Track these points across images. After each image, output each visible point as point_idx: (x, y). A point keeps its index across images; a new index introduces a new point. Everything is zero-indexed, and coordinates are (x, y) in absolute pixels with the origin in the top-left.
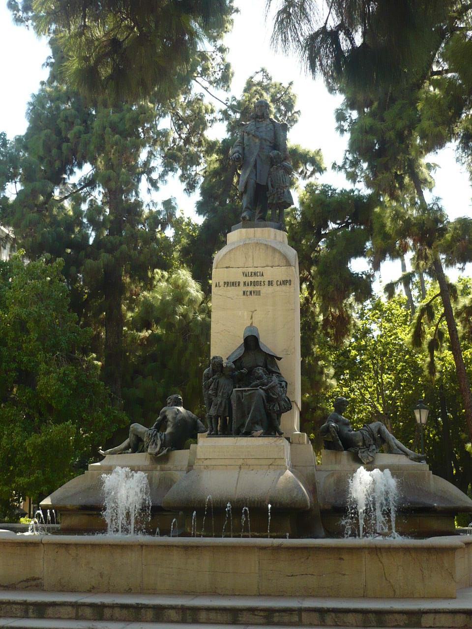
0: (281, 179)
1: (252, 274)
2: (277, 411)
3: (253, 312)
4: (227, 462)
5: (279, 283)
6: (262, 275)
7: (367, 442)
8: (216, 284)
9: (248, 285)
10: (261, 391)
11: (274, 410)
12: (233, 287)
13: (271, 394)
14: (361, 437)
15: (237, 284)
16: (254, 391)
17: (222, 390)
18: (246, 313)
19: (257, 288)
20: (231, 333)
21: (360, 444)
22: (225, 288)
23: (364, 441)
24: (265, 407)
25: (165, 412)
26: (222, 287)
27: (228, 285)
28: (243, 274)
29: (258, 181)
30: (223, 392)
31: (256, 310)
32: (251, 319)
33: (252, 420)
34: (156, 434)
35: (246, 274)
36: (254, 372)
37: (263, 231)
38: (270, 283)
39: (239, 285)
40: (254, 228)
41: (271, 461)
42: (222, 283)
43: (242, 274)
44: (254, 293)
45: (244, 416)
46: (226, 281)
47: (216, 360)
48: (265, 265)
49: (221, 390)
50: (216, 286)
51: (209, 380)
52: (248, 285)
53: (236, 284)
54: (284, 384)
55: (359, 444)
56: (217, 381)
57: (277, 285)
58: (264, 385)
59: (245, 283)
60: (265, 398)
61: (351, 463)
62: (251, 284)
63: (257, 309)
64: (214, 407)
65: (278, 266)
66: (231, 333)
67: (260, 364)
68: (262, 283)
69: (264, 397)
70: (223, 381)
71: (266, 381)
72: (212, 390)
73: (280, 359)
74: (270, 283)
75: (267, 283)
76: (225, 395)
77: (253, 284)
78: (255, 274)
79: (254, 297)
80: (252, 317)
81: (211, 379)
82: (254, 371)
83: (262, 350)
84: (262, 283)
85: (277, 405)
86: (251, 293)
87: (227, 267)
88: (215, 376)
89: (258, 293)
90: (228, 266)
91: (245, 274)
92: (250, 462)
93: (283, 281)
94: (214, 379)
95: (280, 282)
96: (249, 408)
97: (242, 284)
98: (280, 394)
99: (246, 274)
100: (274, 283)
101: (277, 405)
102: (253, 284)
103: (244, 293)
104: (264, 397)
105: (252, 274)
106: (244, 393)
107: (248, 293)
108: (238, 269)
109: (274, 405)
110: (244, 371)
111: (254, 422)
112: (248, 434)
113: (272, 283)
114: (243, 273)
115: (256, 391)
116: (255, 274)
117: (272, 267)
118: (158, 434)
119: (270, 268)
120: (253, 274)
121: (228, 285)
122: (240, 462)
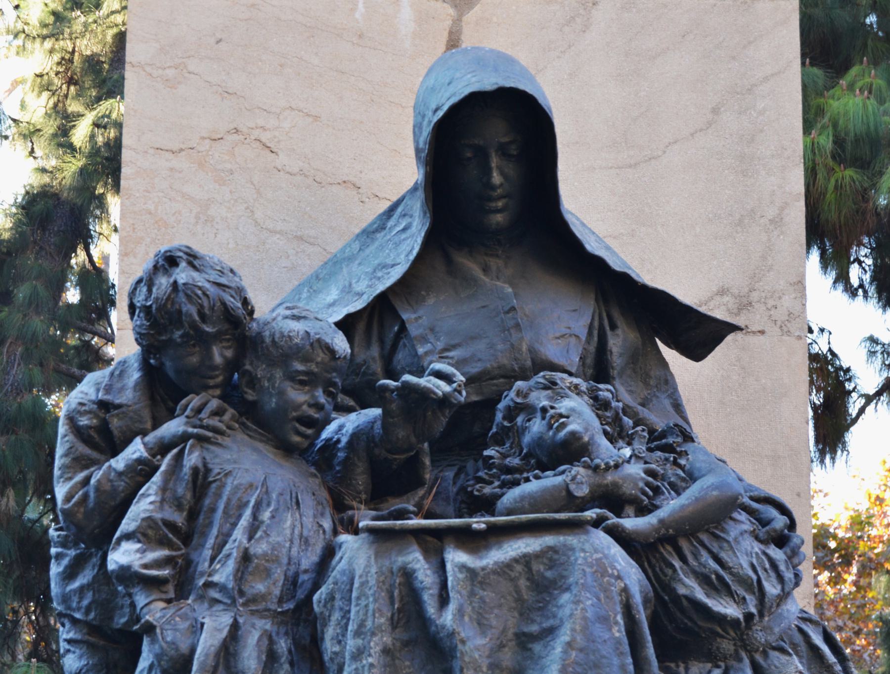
16: (550, 540)
17: (239, 534)
20: (282, 160)
30: (246, 557)
36: (512, 412)
47: (183, 274)
49: (224, 539)
51: (119, 463)
54: (780, 522)
56: (192, 459)
66: (282, 160)
67: (552, 351)
69: (637, 599)
71: (635, 470)
76: (260, 587)
81: (136, 449)
82: (510, 397)
88: (173, 427)
98: (772, 589)
104: (637, 599)
106: (456, 557)
115: (571, 540)
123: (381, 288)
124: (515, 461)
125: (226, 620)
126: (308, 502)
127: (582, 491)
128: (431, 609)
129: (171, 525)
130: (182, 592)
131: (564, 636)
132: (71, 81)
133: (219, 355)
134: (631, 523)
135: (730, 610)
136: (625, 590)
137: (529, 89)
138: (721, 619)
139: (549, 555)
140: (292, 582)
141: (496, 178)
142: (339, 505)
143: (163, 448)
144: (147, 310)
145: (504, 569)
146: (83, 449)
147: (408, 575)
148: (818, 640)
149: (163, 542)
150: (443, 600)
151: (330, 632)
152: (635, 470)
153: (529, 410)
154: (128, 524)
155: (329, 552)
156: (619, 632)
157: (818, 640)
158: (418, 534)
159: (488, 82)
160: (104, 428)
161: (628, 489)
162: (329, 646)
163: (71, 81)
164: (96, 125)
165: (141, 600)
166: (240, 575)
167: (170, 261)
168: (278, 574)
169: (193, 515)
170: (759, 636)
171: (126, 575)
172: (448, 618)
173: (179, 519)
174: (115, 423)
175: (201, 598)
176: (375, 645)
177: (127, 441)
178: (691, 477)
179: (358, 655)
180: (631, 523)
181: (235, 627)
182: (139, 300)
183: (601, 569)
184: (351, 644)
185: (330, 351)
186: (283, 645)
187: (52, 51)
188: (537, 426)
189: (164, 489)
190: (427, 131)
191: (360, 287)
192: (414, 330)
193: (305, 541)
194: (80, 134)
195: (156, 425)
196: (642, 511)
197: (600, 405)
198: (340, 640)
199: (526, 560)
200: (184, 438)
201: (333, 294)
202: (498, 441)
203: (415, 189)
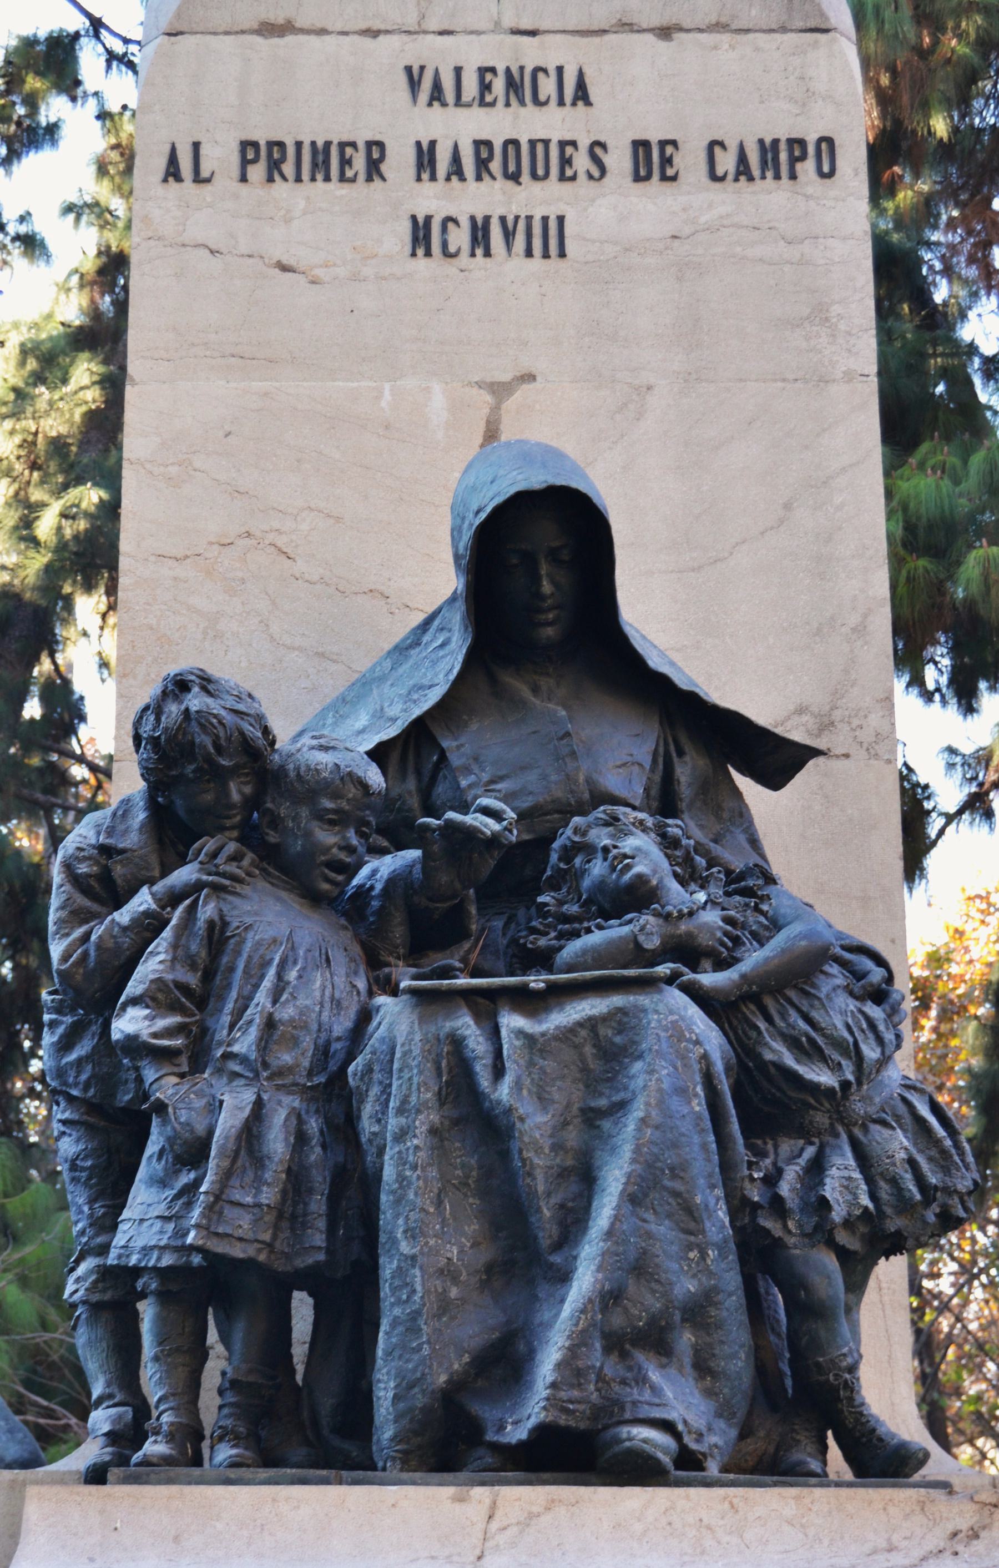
2: (848, 1224)
3: (500, 390)
5: (727, 162)
6: (582, 94)
8: (173, 160)
11: (824, 1205)
12: (320, 184)
15: (359, 163)
16: (617, 1000)
17: (262, 997)
18: (438, 402)
20: (300, 566)
24: (727, 1167)
28: (414, 83)
30: (270, 1024)
35: (437, 87)
36: (569, 853)
39: (374, 169)
43: (403, 79)
44: (509, 235)
47: (195, 701)
48: (601, 18)
49: (244, 1003)
50: (172, 172)
51: (123, 916)
53: (345, 162)
54: (877, 974)
56: (207, 911)
60: (725, 1086)
62: (482, 165)
63: (539, 366)
64: (163, 1183)
65: (719, 27)
66: (300, 566)
67: (612, 782)
68: (582, 162)
69: (719, 1067)
71: (712, 917)
76: (287, 1058)
77: (495, 166)
81: (143, 900)
82: (567, 835)
84: (582, 162)
87: (269, 29)
88: (184, 875)
90: (278, 17)
93: (769, 150)
95: (742, 158)
98: (871, 1052)
99: (437, 87)
102: (495, 166)
104: (719, 1067)
105: (485, 87)
106: (511, 1021)
107: (460, 238)
108: (367, 42)
109: (817, 1168)
113: (667, 161)
114: (413, 79)
116: (513, 85)
117: (665, 32)
119: (650, 37)
120: (499, 85)
121: (274, 167)
123: (417, 712)
124: (574, 909)
125: (249, 1096)
126: (339, 960)
127: (652, 943)
128: (484, 1081)
129: (183, 988)
130: (197, 1066)
131: (637, 1112)
132: (34, 466)
133: (236, 791)
134: (709, 979)
135: (824, 1077)
136: (705, 1057)
138: (814, 1088)
139: (618, 1018)
140: (323, 1052)
141: (547, 588)
142: (373, 962)
143: (173, 899)
144: (155, 741)
145: (567, 1035)
146: (82, 901)
147: (457, 1042)
148: (924, 1111)
149: (174, 1007)
150: (498, 1071)
151: (368, 1109)
152: (712, 917)
153: (588, 850)
154: (134, 987)
155: (365, 1016)
156: (699, 1105)
157: (924, 1111)
158: (468, 995)
159: (536, 479)
160: (105, 877)
161: (705, 940)
162: (367, 1126)
163: (34, 466)
164: (64, 515)
165: (150, 1074)
166: (264, 1043)
168: (307, 1042)
169: (208, 975)
170: (859, 1108)
171: (133, 1045)
172: (504, 1092)
173: (193, 980)
174: (119, 871)
175: (219, 1071)
176: (421, 1124)
177: (132, 892)
178: (776, 925)
179: (401, 1136)
180: (709, 979)
181: (259, 1104)
182: (147, 729)
183: (678, 1033)
184: (393, 1123)
185: (364, 786)
186: (314, 1125)
187: (12, 432)
188: (598, 868)
189: (175, 946)
190: (467, 536)
191: (393, 711)
192: (455, 760)
193: (337, 1004)
194: (45, 526)
195: (164, 874)
196: (721, 964)
197: (669, 843)
198: (379, 1119)
199: (591, 1024)
200: (197, 887)
201: (362, 720)
202: (554, 885)
203: (453, 599)
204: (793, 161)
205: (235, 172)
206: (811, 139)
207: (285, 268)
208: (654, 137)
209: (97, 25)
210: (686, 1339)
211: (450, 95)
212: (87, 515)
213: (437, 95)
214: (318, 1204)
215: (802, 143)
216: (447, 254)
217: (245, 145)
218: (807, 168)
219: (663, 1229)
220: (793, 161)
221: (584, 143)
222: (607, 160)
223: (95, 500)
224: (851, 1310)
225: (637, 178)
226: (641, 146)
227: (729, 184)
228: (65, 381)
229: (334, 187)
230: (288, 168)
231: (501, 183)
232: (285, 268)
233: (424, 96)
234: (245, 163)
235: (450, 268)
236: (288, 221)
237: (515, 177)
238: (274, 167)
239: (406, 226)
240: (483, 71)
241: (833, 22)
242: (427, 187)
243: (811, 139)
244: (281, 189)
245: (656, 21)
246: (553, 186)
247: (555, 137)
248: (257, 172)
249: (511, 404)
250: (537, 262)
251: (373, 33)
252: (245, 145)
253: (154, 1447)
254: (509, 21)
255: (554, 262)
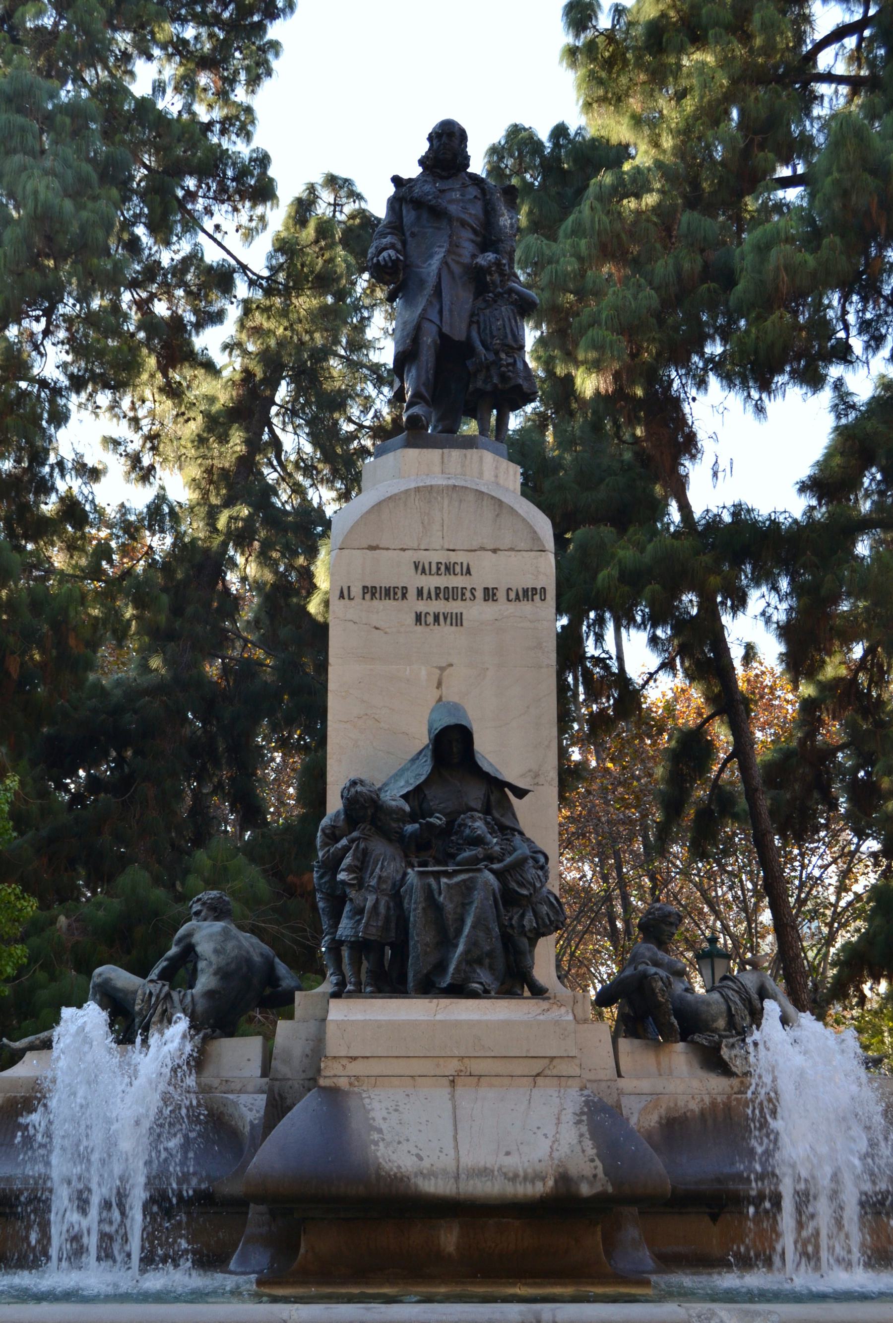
0: (508, 330)
1: (439, 569)
2: (530, 931)
3: (442, 669)
4: (416, 1067)
5: (512, 595)
6: (468, 572)
7: (738, 1019)
8: (342, 592)
9: (429, 597)
10: (491, 877)
11: (524, 926)
12: (387, 601)
13: (514, 885)
14: (724, 1007)
15: (399, 594)
16: (471, 875)
17: (377, 870)
18: (423, 672)
19: (454, 607)
21: (721, 1023)
22: (367, 602)
23: (730, 1016)
24: (498, 916)
25: (189, 935)
26: (358, 600)
27: (373, 595)
28: (416, 567)
29: (446, 330)
30: (380, 877)
31: (451, 665)
32: (438, 688)
33: (467, 952)
34: (168, 996)
35: (424, 568)
36: (460, 825)
37: (465, 456)
38: (490, 594)
39: (404, 596)
40: (442, 448)
41: (538, 1066)
42: (356, 591)
44: (445, 619)
45: (446, 941)
46: (369, 585)
47: (359, 788)
48: (475, 545)
50: (342, 596)
51: (339, 845)
52: (429, 597)
53: (395, 594)
54: (542, 860)
55: (715, 1025)
56: (362, 845)
57: (508, 600)
58: (491, 858)
59: (420, 592)
60: (498, 897)
61: (701, 1073)
62: (437, 595)
64: (350, 918)
65: (511, 549)
67: (473, 804)
69: (497, 891)
70: (380, 848)
71: (497, 848)
72: (349, 869)
73: (521, 793)
74: (490, 594)
75: (479, 594)
76: (384, 886)
77: (441, 595)
78: (449, 569)
79: (446, 630)
80: (439, 685)
81: (344, 842)
82: (459, 821)
83: (479, 769)
84: (468, 595)
85: (529, 915)
86: (436, 618)
88: (355, 834)
89: (457, 620)
90: (374, 544)
91: (420, 568)
92: (478, 1067)
93: (526, 591)
94: (352, 841)
95: (517, 594)
96: (462, 921)
97: (412, 593)
98: (538, 885)
99: (424, 568)
100: (501, 595)
101: (529, 915)
103: (418, 618)
105: (439, 569)
106: (444, 880)
107: (430, 619)
108: (402, 553)
109: (522, 916)
110: (438, 820)
111: (472, 960)
112: (458, 991)
113: (494, 595)
115: (478, 875)
116: (447, 568)
117: (495, 551)
118: (175, 995)
120: (443, 568)
122: (451, 1067)
123: (418, 783)
124: (461, 842)
125: (374, 897)
126: (398, 859)
127: (481, 856)
128: (436, 896)
129: (356, 866)
130: (360, 889)
131: (475, 905)
132: (211, 482)
133: (369, 812)
134: (495, 866)
136: (494, 890)
137: (464, 723)
138: (523, 895)
139: (471, 879)
140: (394, 884)
141: (455, 750)
142: (406, 856)
143: (352, 841)
144: (347, 799)
145: (457, 884)
146: (327, 840)
147: (429, 885)
148: (552, 900)
149: (354, 872)
150: (440, 894)
151: (406, 901)
152: (497, 848)
153: (465, 825)
154: (343, 866)
155: (405, 874)
156: (491, 902)
157: (552, 900)
158: (432, 873)
159: (452, 721)
160: (333, 833)
161: (495, 855)
162: (406, 905)
163: (211, 482)
164: (231, 518)
165: (348, 890)
166: (378, 882)
167: (354, 783)
168: (390, 882)
169: (363, 863)
170: (534, 899)
171: (343, 882)
172: (441, 899)
173: (358, 864)
174: (337, 832)
175: (367, 889)
176: (420, 907)
177: (341, 838)
178: (515, 850)
179: (415, 910)
180: (495, 866)
181: (377, 899)
182: (345, 795)
183: (486, 883)
184: (413, 906)
185: (404, 811)
186: (392, 904)
187: (200, 465)
188: (467, 831)
189: (354, 855)
190: (432, 736)
191: (411, 781)
192: (429, 797)
193: (397, 871)
194: (222, 522)
195: (350, 833)
196: (500, 861)
197: (487, 823)
198: (409, 903)
199: (464, 881)
200: (358, 839)
201: (402, 783)
202: (456, 833)
203: (427, 746)
204: (533, 595)
205: (361, 596)
206: (539, 587)
207: (377, 628)
208: (490, 586)
209: (244, 268)
210: (487, 961)
211: (427, 572)
212: (242, 519)
213: (423, 571)
214: (393, 925)
215: (536, 589)
216: (426, 625)
217: (365, 587)
218: (537, 597)
219: (481, 934)
220: (533, 595)
221: (469, 588)
222: (476, 594)
223: (246, 512)
224: (532, 952)
225: (485, 600)
226: (486, 589)
227: (513, 603)
228: (228, 442)
229: (392, 602)
230: (377, 595)
231: (443, 602)
232: (377, 628)
233: (419, 571)
234: (364, 593)
235: (427, 629)
236: (377, 613)
237: (447, 599)
238: (373, 595)
239: (414, 615)
240: (438, 563)
241: (547, 548)
242: (420, 602)
243: (539, 587)
244: (375, 602)
245: (492, 547)
246: (459, 602)
247: (460, 586)
248: (368, 596)
249: (446, 673)
250: (454, 628)
251: (403, 550)
252: (365, 587)
253: (349, 987)
254: (446, 547)
255: (459, 628)
